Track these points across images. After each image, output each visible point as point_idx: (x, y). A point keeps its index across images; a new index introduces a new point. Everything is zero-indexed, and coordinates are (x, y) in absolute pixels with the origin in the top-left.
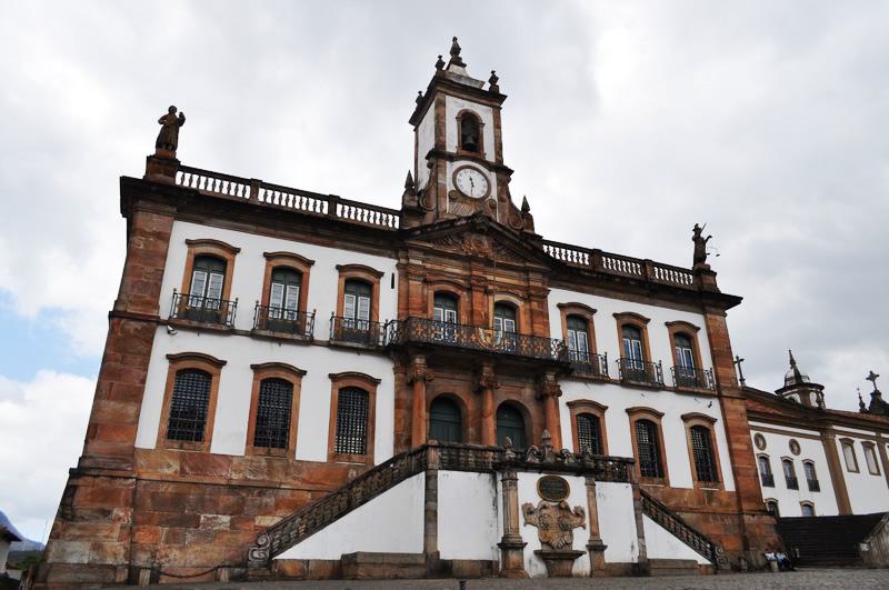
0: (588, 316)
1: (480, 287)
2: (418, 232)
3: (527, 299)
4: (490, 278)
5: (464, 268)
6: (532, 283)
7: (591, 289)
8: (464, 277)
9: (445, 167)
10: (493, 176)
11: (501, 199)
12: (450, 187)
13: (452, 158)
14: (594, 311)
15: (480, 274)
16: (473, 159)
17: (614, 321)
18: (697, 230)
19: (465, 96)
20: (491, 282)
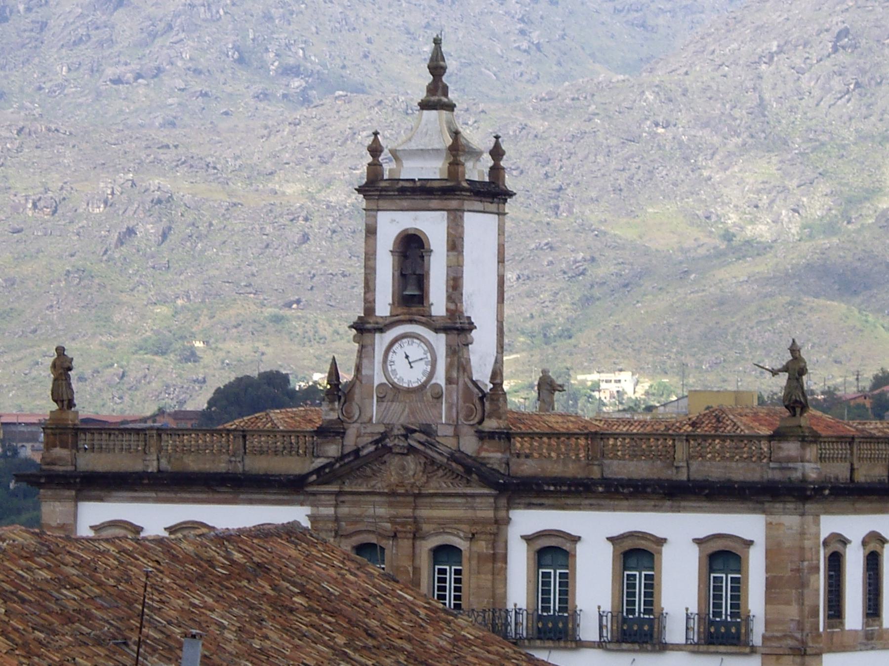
0: (567, 546)
1: (405, 532)
2: (314, 477)
3: (472, 538)
4: (424, 513)
5: (391, 505)
6: (480, 514)
7: (577, 501)
8: (392, 520)
9: (373, 345)
10: (440, 342)
11: (449, 381)
12: (379, 379)
13: (381, 330)
14: (576, 539)
15: (408, 512)
16: (411, 321)
17: (609, 547)
18: (794, 350)
19: (405, 203)
20: (429, 520)
